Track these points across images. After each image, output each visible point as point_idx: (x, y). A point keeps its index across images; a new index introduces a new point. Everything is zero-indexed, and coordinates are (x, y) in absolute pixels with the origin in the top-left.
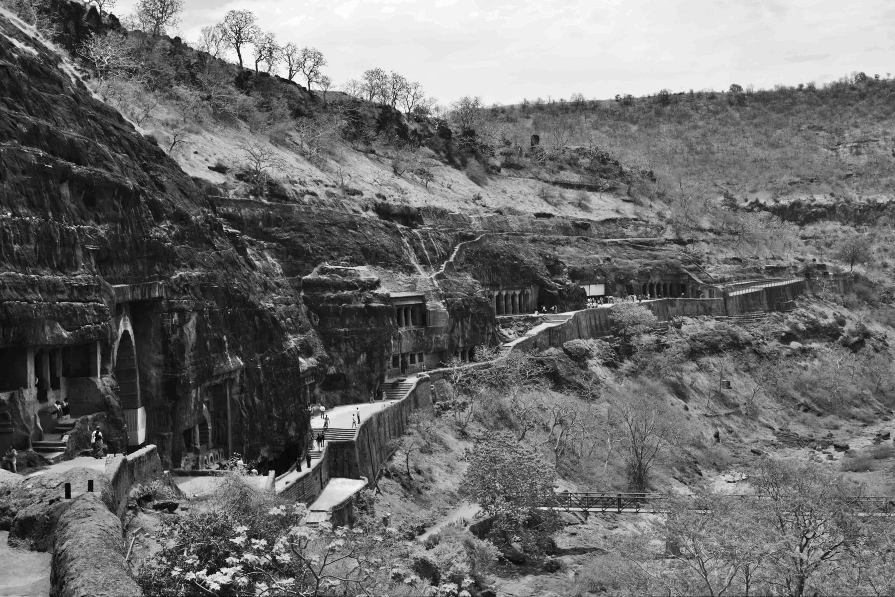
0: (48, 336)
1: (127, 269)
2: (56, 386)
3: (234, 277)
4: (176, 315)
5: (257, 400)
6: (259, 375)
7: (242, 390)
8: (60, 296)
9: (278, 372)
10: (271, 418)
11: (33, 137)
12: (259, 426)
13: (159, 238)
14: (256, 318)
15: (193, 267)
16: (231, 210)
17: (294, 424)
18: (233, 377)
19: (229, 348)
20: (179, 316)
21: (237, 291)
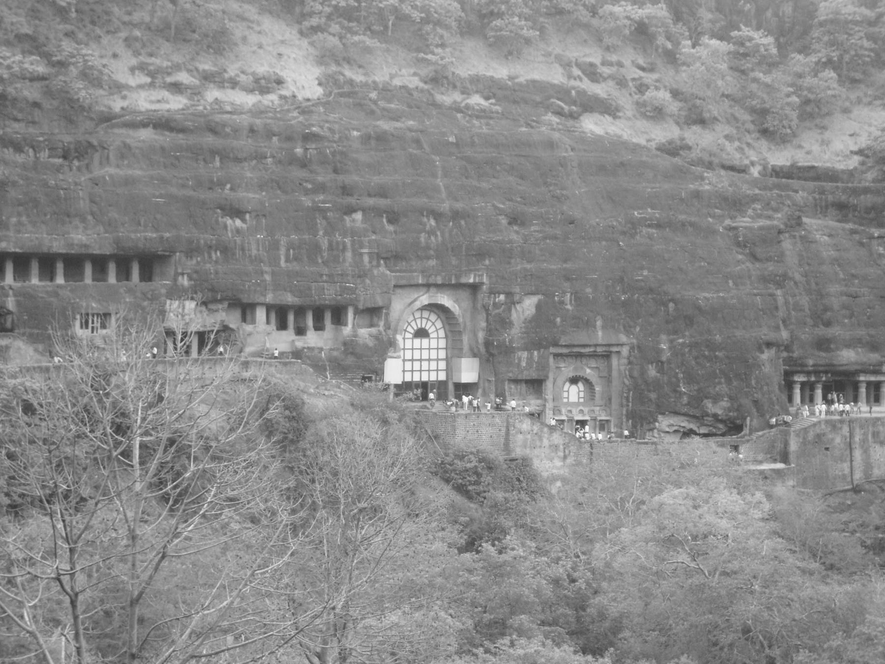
0: (269, 298)
1: (432, 263)
2: (319, 327)
3: (642, 268)
4: (502, 297)
5: (652, 372)
6: (659, 351)
7: (630, 363)
8: (299, 279)
9: (695, 353)
10: (675, 391)
11: (321, 188)
12: (653, 396)
13: (497, 242)
14: (671, 305)
15: (565, 261)
16: (843, 198)
17: (725, 403)
18: (614, 349)
19: (604, 327)
20: (506, 297)
21: (637, 281)
